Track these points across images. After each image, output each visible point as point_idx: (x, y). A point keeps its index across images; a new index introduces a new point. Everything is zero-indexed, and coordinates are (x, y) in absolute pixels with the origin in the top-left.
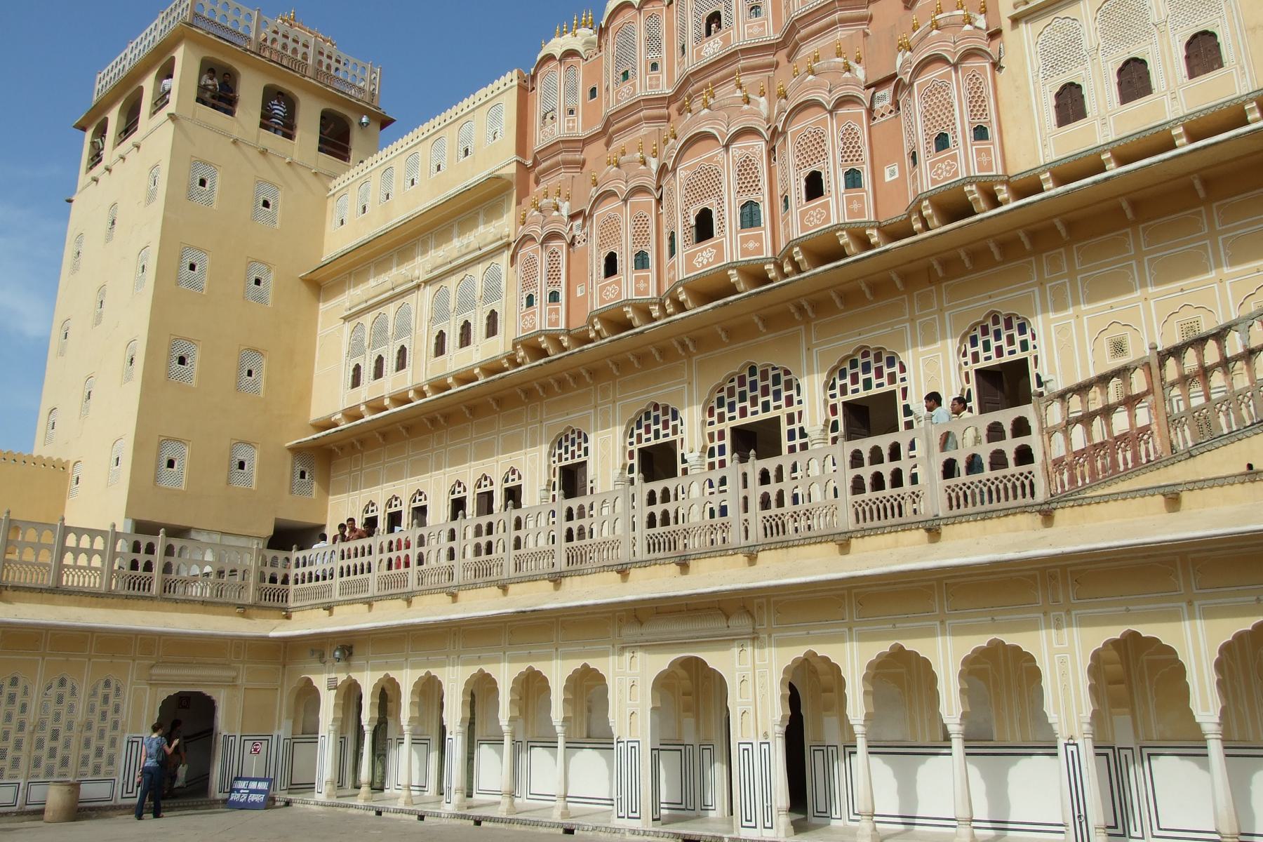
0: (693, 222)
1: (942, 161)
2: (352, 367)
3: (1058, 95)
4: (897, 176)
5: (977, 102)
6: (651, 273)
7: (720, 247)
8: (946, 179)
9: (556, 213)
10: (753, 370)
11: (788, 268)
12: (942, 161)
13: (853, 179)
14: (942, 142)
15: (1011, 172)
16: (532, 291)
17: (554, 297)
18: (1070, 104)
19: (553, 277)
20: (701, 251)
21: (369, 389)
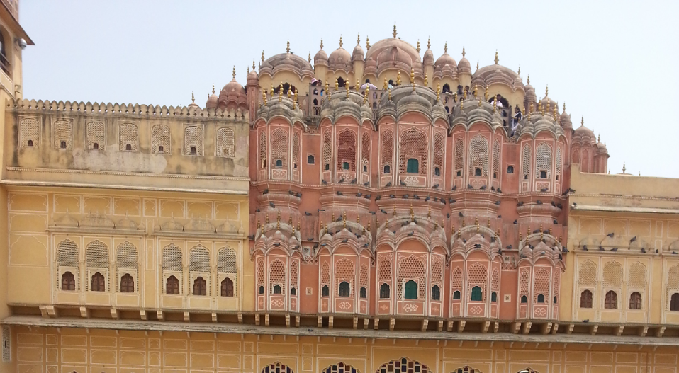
0: (404, 286)
1: (541, 307)
2: (63, 270)
3: (582, 293)
4: (509, 300)
5: (556, 284)
6: (367, 301)
7: (420, 306)
8: (541, 316)
9: (294, 237)
10: (404, 361)
11: (450, 325)
12: (541, 307)
13: (494, 299)
14: (541, 299)
15: (563, 320)
16: (280, 284)
17: (294, 291)
18: (586, 299)
19: (294, 281)
20: (409, 304)
21: (83, 296)
